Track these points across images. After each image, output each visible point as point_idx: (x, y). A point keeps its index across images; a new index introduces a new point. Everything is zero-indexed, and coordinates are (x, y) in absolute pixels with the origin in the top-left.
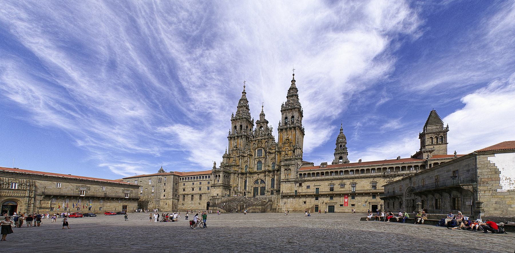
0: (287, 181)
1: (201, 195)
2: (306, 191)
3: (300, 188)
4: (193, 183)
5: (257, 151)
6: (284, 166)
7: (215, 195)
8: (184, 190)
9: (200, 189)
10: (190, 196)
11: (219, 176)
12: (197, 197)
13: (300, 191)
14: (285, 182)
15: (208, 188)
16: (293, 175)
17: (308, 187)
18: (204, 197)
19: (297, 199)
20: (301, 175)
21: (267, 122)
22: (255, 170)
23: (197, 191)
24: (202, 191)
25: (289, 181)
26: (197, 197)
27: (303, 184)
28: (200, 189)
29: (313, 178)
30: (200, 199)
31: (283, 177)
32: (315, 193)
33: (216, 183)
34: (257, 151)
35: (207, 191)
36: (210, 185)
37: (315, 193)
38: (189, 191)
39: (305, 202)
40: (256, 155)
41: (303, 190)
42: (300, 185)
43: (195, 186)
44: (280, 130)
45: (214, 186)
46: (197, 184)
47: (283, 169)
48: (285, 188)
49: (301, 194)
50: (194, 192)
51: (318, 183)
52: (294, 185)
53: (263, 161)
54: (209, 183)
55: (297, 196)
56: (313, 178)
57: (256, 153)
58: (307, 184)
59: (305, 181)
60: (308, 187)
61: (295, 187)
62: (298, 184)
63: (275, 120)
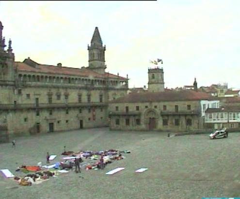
17: (28, 95)
19: (18, 114)
20: (20, 75)
25: (7, 85)
27: (23, 92)
29: (34, 83)
42: (20, 92)
49: (22, 106)
51: (38, 91)
52: (12, 91)
59: (25, 86)
60: (28, 95)
62: (16, 91)
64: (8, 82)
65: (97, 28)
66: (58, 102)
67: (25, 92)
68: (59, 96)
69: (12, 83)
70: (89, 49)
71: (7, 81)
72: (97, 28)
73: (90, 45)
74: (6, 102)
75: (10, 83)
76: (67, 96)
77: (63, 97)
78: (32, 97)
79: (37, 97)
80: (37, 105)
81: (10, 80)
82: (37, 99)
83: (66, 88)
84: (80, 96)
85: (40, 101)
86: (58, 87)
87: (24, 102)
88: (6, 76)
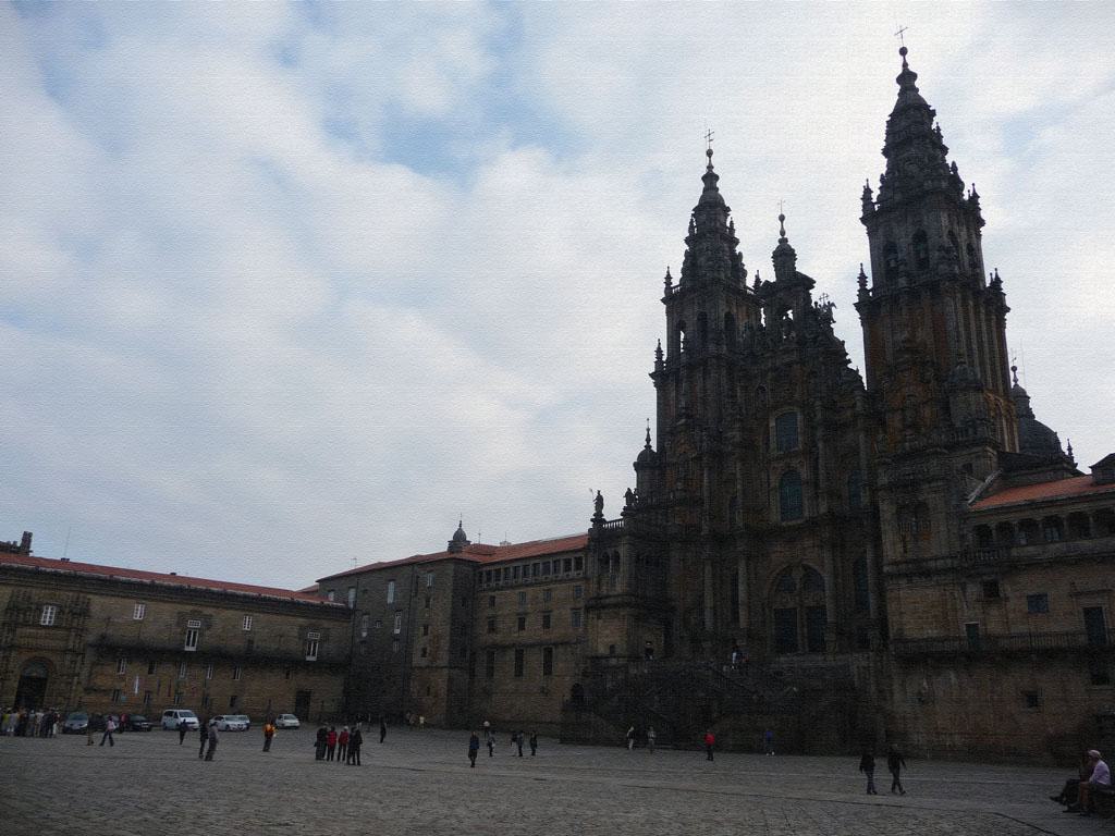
0: (918, 571)
1: (549, 653)
2: (1022, 628)
3: (994, 612)
4: (523, 595)
5: (772, 424)
6: (890, 488)
7: (602, 650)
8: (492, 629)
9: (546, 625)
10: (511, 655)
11: (617, 557)
12: (534, 660)
13: (994, 627)
14: (908, 576)
15: (576, 623)
16: (940, 543)
17: (1037, 603)
20: (983, 532)
21: (808, 283)
22: (775, 517)
23: (534, 631)
24: (556, 633)
25: (927, 574)
26: (534, 660)
27: (1006, 588)
28: (546, 625)
30: (548, 670)
31: (892, 549)
32: (1083, 639)
34: (772, 424)
36: (582, 604)
37: (1083, 639)
38: (507, 632)
39: (1032, 699)
40: (773, 445)
41: (1008, 620)
42: (992, 593)
44: (868, 307)
45: (596, 606)
47: (887, 510)
48: (915, 612)
49: (1004, 643)
50: (526, 636)
53: (804, 473)
54: (578, 589)
55: (975, 654)
56: (1056, 548)
57: (772, 433)
58: (1031, 583)
59: (1014, 568)
60: (1037, 603)
61: (968, 609)
62: (974, 590)
63: (839, 265)
64: (932, 564)
67: (1016, 593)
71: (926, 560)
74: (932, 632)
75: (940, 563)
79: (1087, 602)
81: (945, 551)
87: (1014, 630)
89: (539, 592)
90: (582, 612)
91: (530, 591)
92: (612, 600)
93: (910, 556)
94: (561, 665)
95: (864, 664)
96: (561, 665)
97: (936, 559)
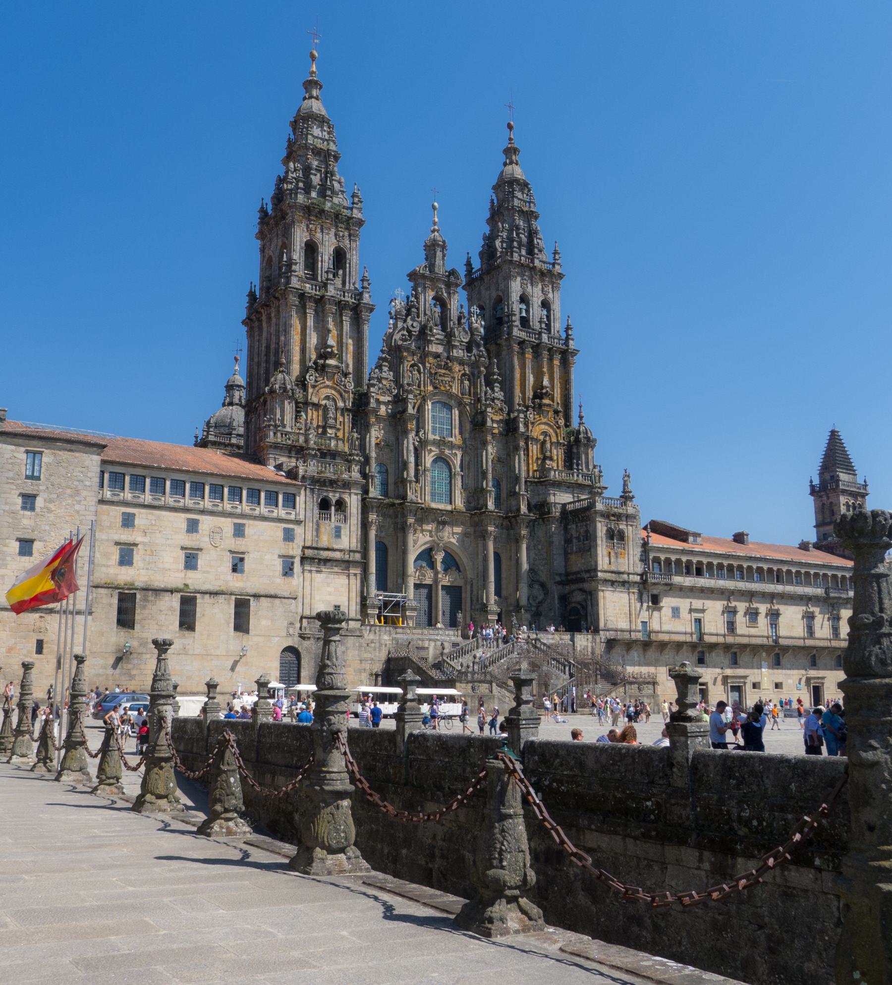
3: (656, 614)
10: (174, 602)
11: (341, 505)
12: (215, 616)
14: (613, 583)
15: (288, 571)
17: (676, 612)
18: (262, 616)
25: (624, 583)
26: (215, 616)
30: (241, 623)
33: (325, 541)
35: (280, 585)
36: (295, 550)
43: (201, 539)
45: (315, 558)
46: (216, 531)
50: (195, 580)
54: (289, 536)
59: (671, 589)
60: (676, 612)
65: (834, 435)
66: (753, 631)
68: (753, 615)
69: (637, 578)
70: (813, 492)
71: (623, 573)
72: (834, 435)
73: (816, 481)
74: (623, 624)
76: (774, 615)
77: (763, 621)
78: (684, 613)
80: (701, 635)
82: (698, 621)
83: (771, 597)
84: (809, 617)
85: (708, 628)
86: (750, 595)
87: (665, 628)
88: (620, 560)
89: (227, 524)
90: (297, 561)
91: (206, 523)
92: (338, 555)
93: (613, 568)
94: (264, 622)
95: (585, 643)
96: (264, 622)
97: (629, 574)
